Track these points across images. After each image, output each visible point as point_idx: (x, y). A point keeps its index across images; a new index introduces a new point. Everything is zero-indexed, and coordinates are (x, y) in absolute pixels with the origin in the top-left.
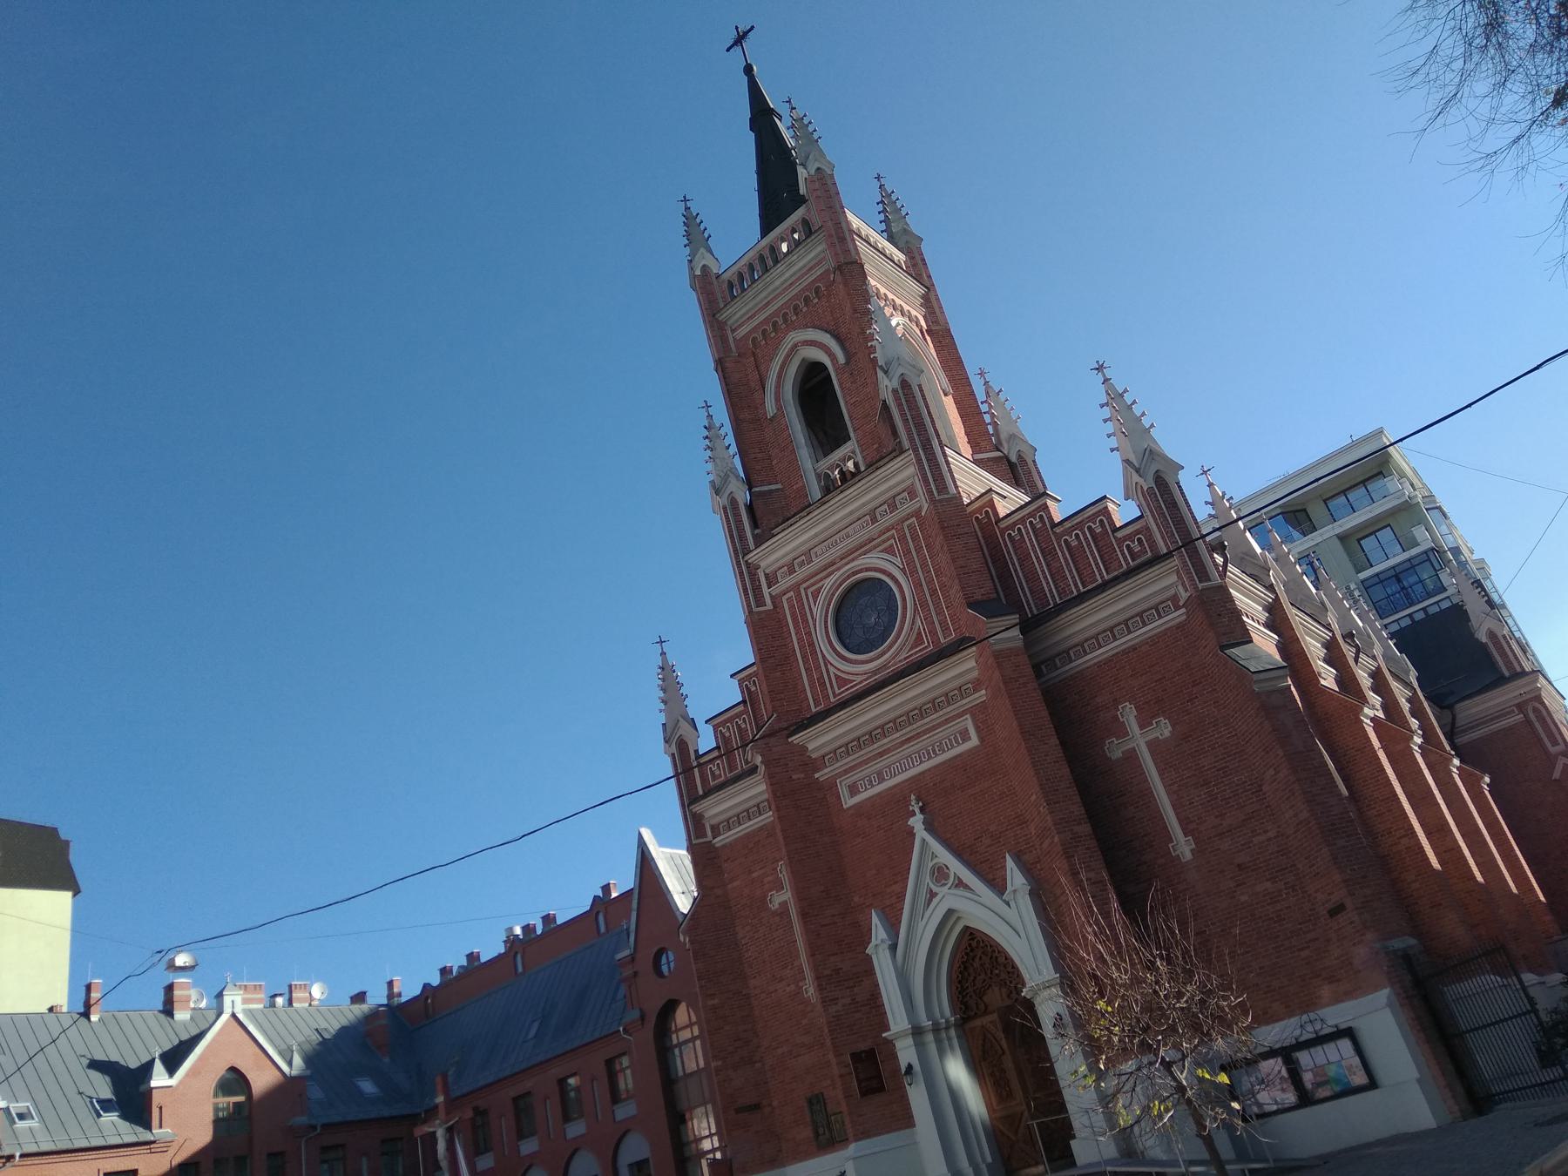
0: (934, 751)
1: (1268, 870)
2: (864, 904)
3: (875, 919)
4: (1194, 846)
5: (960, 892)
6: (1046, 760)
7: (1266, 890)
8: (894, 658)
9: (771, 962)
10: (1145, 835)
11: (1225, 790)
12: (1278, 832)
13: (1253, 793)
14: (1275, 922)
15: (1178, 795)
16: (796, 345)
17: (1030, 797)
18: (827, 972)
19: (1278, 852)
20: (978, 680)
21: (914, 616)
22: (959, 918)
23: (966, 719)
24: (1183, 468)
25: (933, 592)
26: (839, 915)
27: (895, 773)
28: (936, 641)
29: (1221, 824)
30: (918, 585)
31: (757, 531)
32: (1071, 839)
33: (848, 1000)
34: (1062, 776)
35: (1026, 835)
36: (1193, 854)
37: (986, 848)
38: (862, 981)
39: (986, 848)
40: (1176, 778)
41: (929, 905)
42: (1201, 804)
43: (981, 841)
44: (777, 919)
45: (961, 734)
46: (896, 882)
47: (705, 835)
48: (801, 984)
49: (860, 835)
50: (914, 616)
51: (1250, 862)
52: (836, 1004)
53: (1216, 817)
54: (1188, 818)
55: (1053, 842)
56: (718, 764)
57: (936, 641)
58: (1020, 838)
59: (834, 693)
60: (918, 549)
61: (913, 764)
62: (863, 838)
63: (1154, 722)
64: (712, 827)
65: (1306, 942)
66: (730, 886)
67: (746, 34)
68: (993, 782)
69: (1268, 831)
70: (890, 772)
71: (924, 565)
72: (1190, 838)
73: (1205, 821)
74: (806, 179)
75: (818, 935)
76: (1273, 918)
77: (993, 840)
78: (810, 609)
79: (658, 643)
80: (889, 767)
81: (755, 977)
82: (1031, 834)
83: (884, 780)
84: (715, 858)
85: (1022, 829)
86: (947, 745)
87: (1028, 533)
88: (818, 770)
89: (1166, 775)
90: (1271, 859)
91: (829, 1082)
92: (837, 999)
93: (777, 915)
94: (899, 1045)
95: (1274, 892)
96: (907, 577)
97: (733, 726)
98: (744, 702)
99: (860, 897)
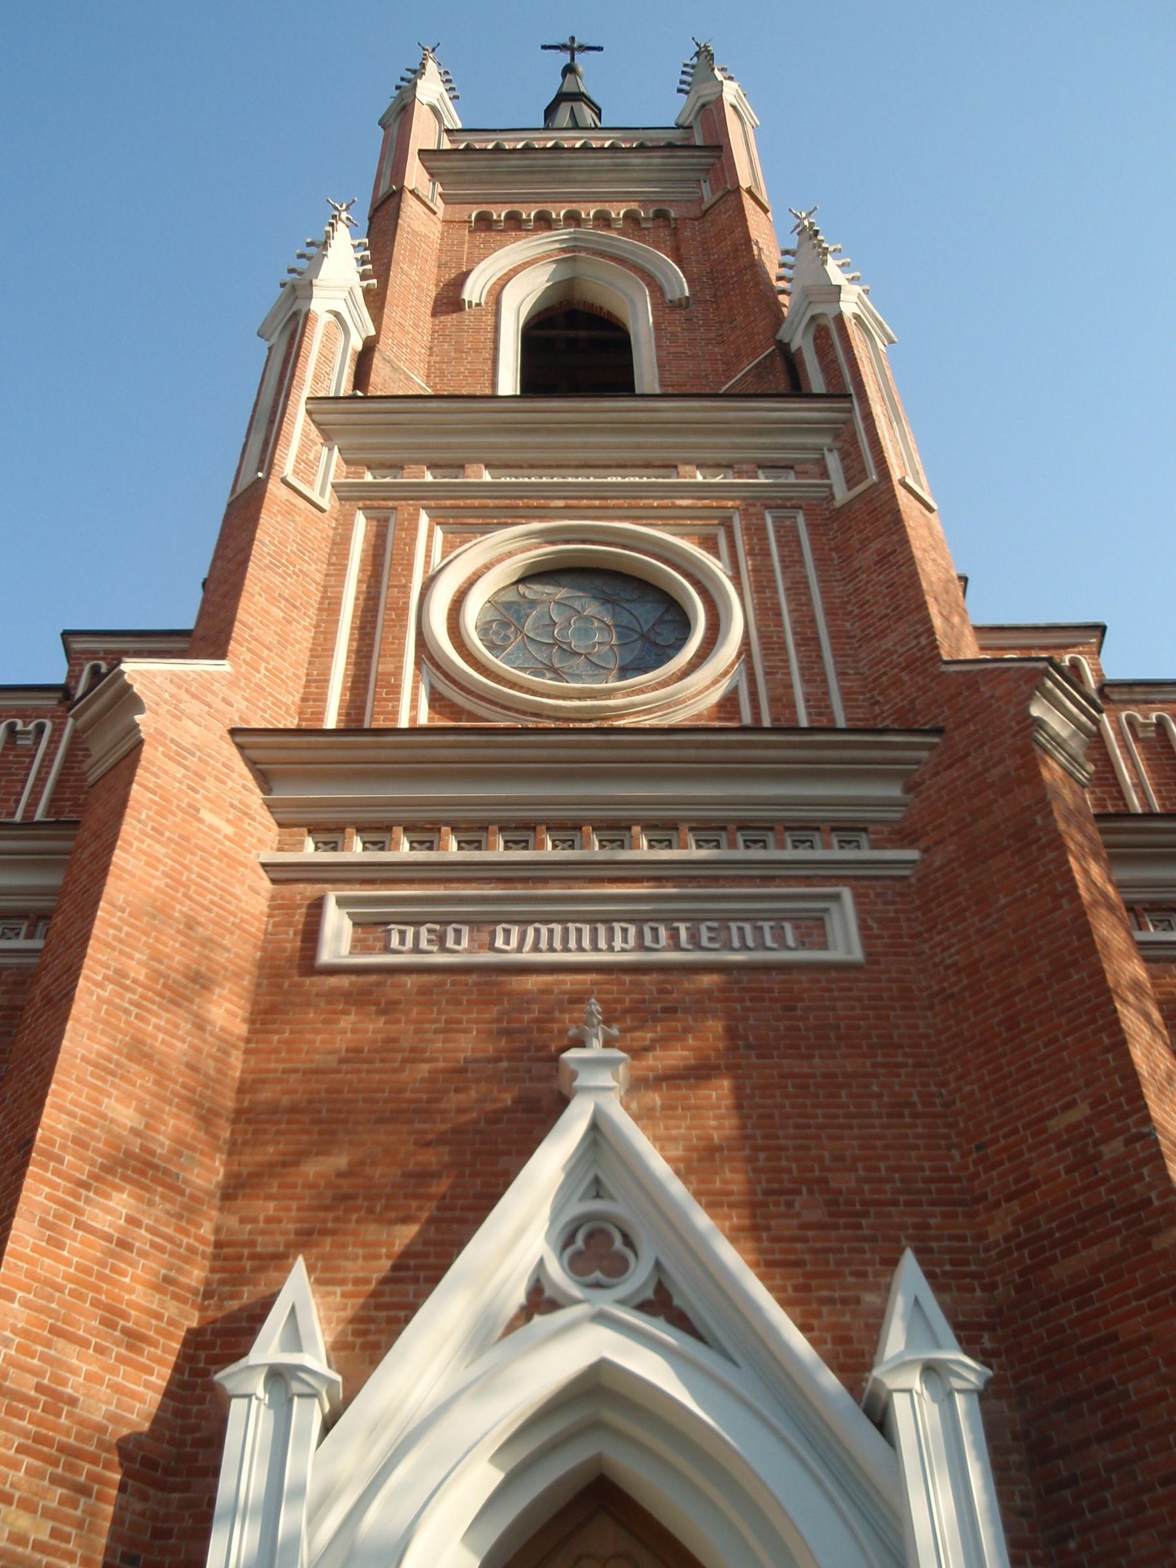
17: (1053, 1113)
23: (836, 897)
25: (808, 641)
30: (766, 612)
35: (963, 1238)
43: (789, 1205)
45: (796, 927)
55: (1148, 1246)
58: (939, 1238)
60: (792, 561)
61: (611, 938)
68: (874, 1065)
77: (831, 1215)
82: (983, 1236)
86: (742, 938)
98: (65, 692)
99: (243, 1221)
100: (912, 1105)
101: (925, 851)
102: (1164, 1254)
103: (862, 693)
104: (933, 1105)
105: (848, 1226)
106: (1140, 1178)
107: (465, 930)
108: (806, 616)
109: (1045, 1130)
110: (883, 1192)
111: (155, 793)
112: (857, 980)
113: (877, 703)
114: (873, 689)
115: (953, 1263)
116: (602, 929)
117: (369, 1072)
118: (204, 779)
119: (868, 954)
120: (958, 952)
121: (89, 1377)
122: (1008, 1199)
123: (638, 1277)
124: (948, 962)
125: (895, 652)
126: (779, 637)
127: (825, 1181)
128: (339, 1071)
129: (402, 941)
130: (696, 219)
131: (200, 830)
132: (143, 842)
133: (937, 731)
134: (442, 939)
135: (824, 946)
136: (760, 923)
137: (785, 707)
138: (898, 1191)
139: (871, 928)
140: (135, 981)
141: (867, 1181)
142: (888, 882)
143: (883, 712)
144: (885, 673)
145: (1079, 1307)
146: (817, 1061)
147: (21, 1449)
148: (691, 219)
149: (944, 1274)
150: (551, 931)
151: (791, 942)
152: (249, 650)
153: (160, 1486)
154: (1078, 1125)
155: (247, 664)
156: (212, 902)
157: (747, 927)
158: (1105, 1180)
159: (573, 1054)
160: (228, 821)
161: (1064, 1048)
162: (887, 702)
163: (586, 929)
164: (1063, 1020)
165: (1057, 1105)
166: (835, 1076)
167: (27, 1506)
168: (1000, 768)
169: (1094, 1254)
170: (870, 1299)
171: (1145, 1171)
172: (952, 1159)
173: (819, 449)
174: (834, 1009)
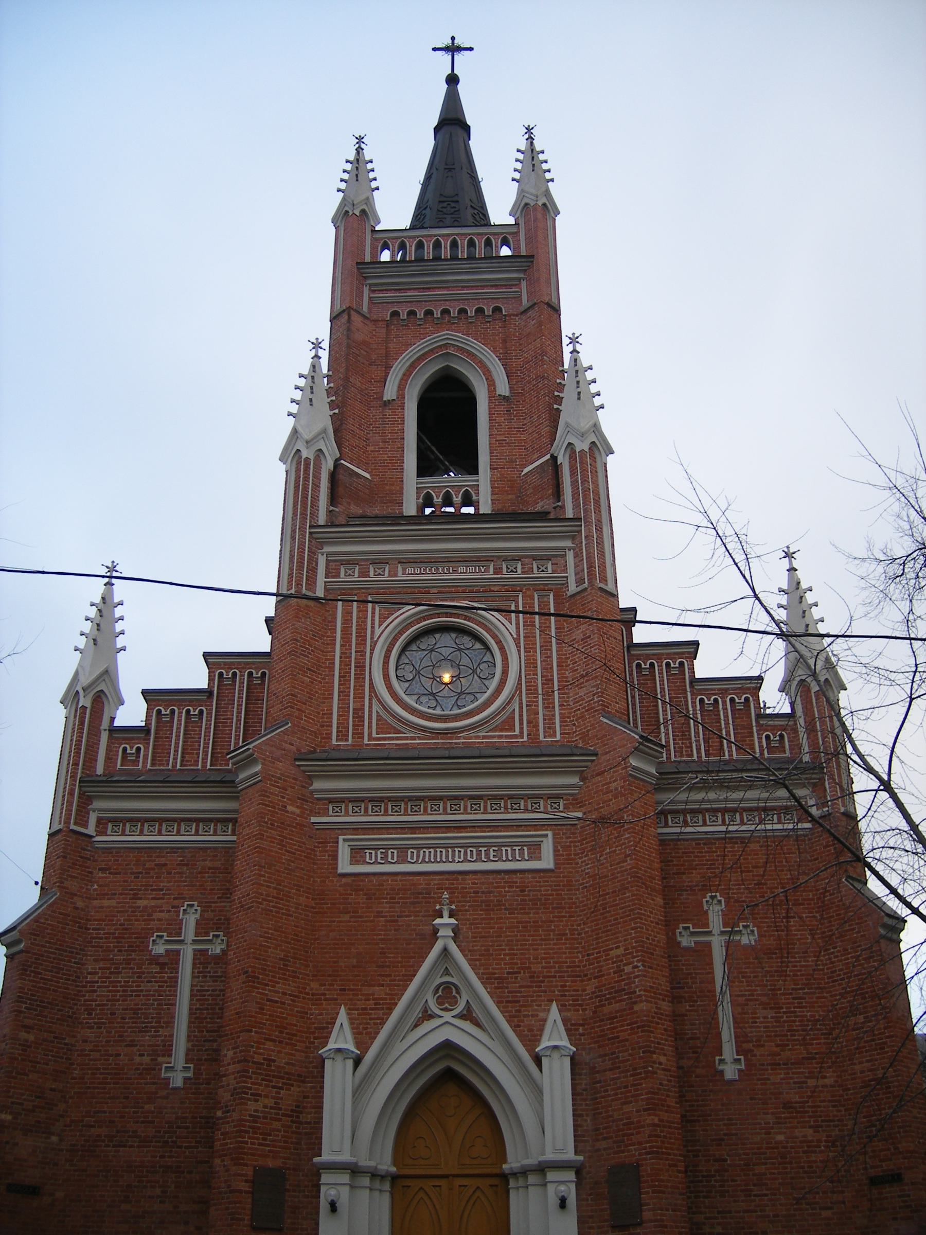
0: (487, 855)
2: (324, 994)
3: (343, 1017)
4: (743, 1067)
5: (467, 1025)
6: (650, 917)
8: (468, 731)
9: (123, 1018)
10: (691, 1039)
11: (795, 1021)
15: (743, 1009)
16: (446, 346)
17: (612, 949)
18: (258, 1058)
19: (830, 1101)
20: (576, 800)
21: (513, 696)
22: (447, 1056)
23: (546, 836)
24: (846, 689)
25: (548, 681)
26: (290, 995)
27: (424, 856)
28: (533, 735)
30: (531, 664)
31: (332, 508)
32: (656, 1013)
33: (270, 1102)
34: (658, 941)
35: (578, 991)
37: (521, 987)
38: (292, 1085)
39: (521, 987)
40: (746, 991)
41: (416, 1026)
42: (765, 1027)
43: (516, 978)
44: (155, 969)
46: (382, 985)
47: (86, 826)
48: (160, 1059)
49: (349, 912)
50: (513, 696)
51: (797, 1102)
52: (257, 1101)
53: (777, 1046)
55: (632, 1008)
56: (139, 749)
57: (533, 735)
59: (370, 734)
61: (453, 856)
62: (351, 917)
63: (741, 924)
64: (99, 821)
66: (95, 903)
67: (459, 49)
69: (825, 1077)
70: (418, 856)
71: (546, 646)
72: (742, 1057)
73: (763, 1046)
74: (526, 204)
75: (263, 1009)
76: (803, 1167)
77: (531, 982)
78: (373, 627)
79: (107, 567)
80: (418, 848)
81: (92, 1028)
82: (584, 990)
83: (403, 860)
84: (89, 859)
85: (572, 981)
86: (507, 854)
87: (661, 673)
88: (318, 814)
89: (737, 983)
90: (819, 1107)
91: (158, 1191)
92: (260, 1095)
93: (157, 964)
94: (325, 1178)
95: (812, 1141)
96: (519, 651)
97: (180, 713)
98: (208, 692)
99: (321, 985)
100: (565, 934)
101: (584, 814)
102: (636, 1012)
103: (569, 717)
104: (574, 934)
105: (536, 987)
106: (634, 982)
107: (395, 852)
108: (548, 664)
109: (608, 955)
110: (551, 972)
111: (269, 806)
112: (551, 877)
113: (574, 725)
114: (573, 717)
115: (573, 1000)
116: (450, 850)
117: (362, 922)
118: (286, 790)
119: (556, 864)
120: (590, 868)
121: (279, 1052)
122: (595, 978)
123: (460, 1007)
124: (587, 871)
125: (584, 699)
126: (534, 682)
127: (530, 968)
128: (350, 922)
129: (371, 858)
130: (517, 315)
131: (287, 816)
132: (267, 832)
133: (596, 755)
134: (387, 856)
135: (539, 859)
136: (514, 848)
137: (534, 727)
138: (556, 972)
139: (559, 851)
140: (273, 897)
141: (546, 967)
142: (569, 827)
143: (576, 731)
144: (579, 709)
145: (610, 1024)
146: (532, 915)
147: (263, 1080)
148: (514, 315)
149: (570, 1005)
150: (430, 852)
151: (526, 857)
152: (298, 709)
153: (304, 1082)
154: (618, 956)
155: (297, 718)
156: (295, 849)
157: (509, 849)
158: (624, 980)
159: (438, 921)
160: (297, 807)
161: (619, 923)
162: (579, 726)
163: (444, 851)
164: (621, 911)
165: (614, 946)
166: (537, 922)
167: (266, 1096)
168: (615, 784)
169: (617, 1006)
170: (542, 1015)
171: (637, 980)
172: (578, 957)
173: (564, 549)
174: (540, 891)
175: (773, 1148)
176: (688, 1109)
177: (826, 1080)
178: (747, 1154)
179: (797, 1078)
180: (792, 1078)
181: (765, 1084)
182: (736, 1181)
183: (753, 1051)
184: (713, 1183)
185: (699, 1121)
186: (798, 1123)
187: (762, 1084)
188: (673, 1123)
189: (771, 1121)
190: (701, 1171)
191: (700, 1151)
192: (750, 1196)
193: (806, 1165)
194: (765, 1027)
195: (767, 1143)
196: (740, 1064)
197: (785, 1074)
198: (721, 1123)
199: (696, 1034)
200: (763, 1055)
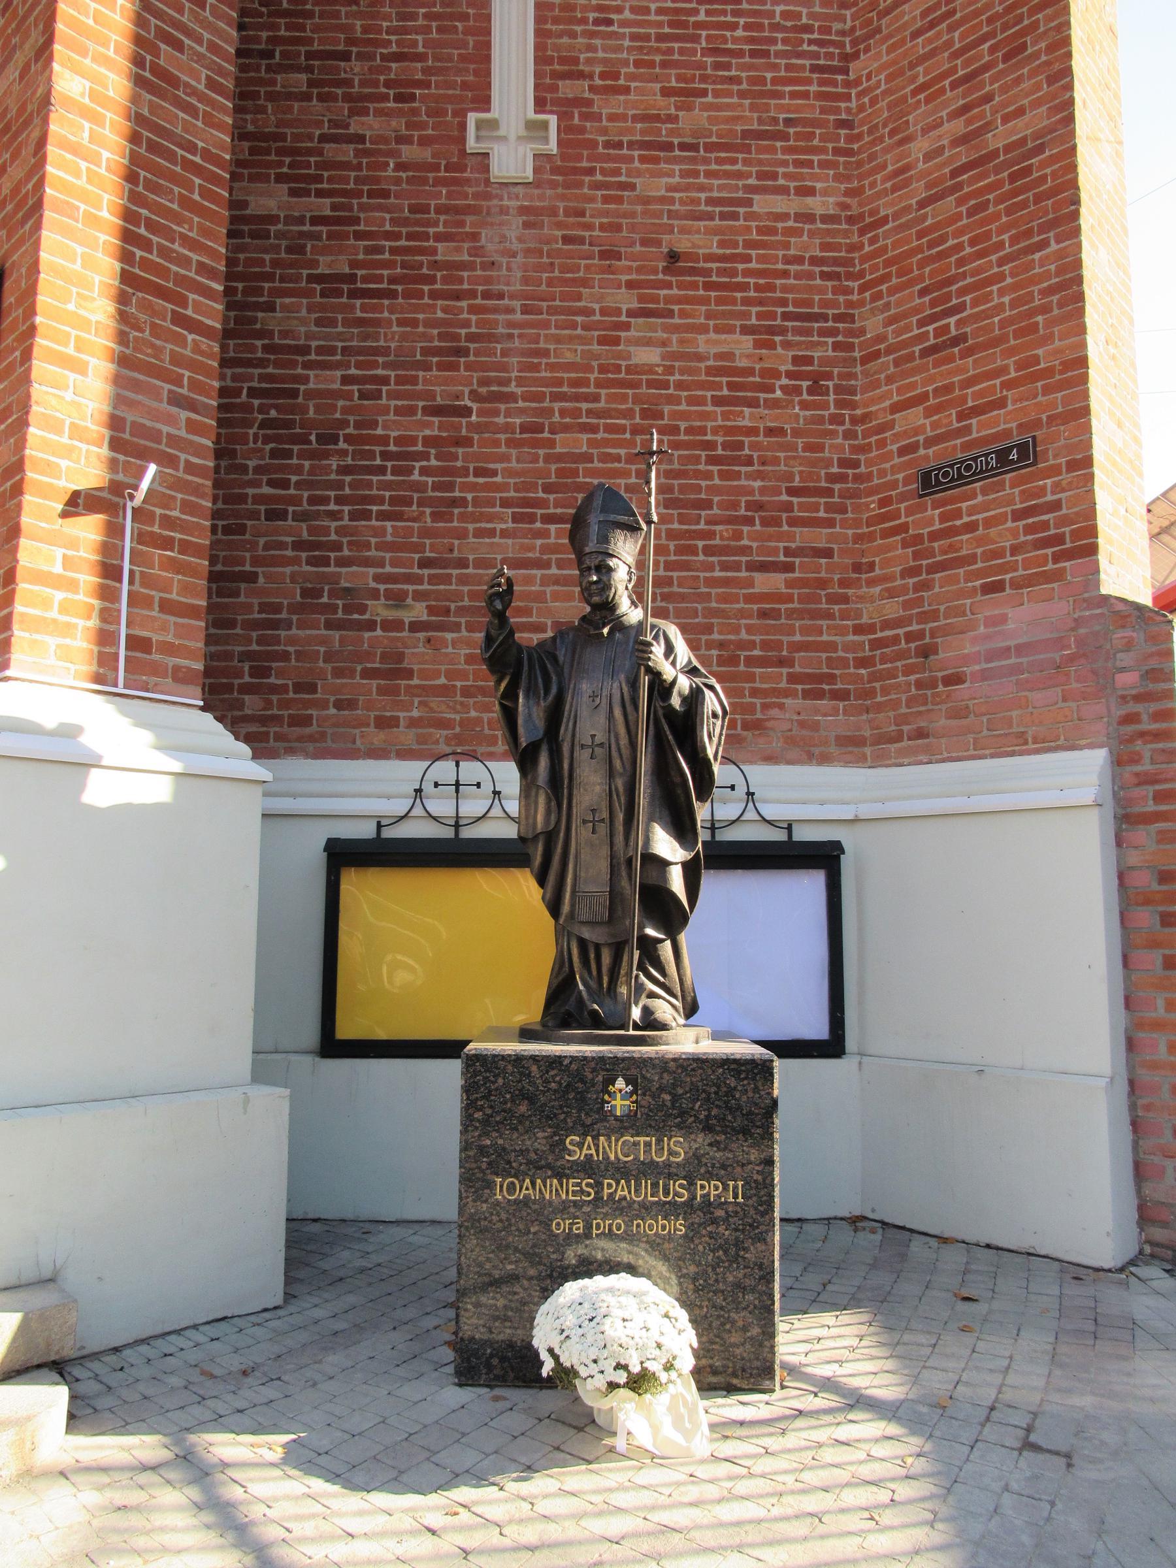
1: (760, 302)
4: (553, 147)
7: (729, 356)
10: (398, 57)
12: (845, 207)
13: (815, 69)
14: (712, 460)
19: (814, 261)
29: (672, 119)
36: (536, 170)
42: (634, 37)
51: (710, 258)
53: (667, 92)
54: (576, 61)
65: (788, 552)
69: (811, 192)
72: (553, 120)
73: (626, 90)
76: (710, 445)
90: (785, 274)
95: (750, 371)
175: (623, 384)
176: (361, 257)
177: (809, 200)
178: (539, 397)
179: (721, 188)
180: (701, 188)
181: (619, 200)
182: (494, 473)
183: (589, 103)
184: (416, 476)
185: (392, 295)
186: (708, 317)
187: (606, 199)
188: (191, 148)
189: (624, 308)
190: (384, 440)
191: (385, 380)
192: (532, 519)
193: (720, 439)
194: (634, 37)
195: (603, 369)
196: (546, 140)
197: (684, 174)
198: (464, 304)
199: (414, 44)
200: (622, 117)
